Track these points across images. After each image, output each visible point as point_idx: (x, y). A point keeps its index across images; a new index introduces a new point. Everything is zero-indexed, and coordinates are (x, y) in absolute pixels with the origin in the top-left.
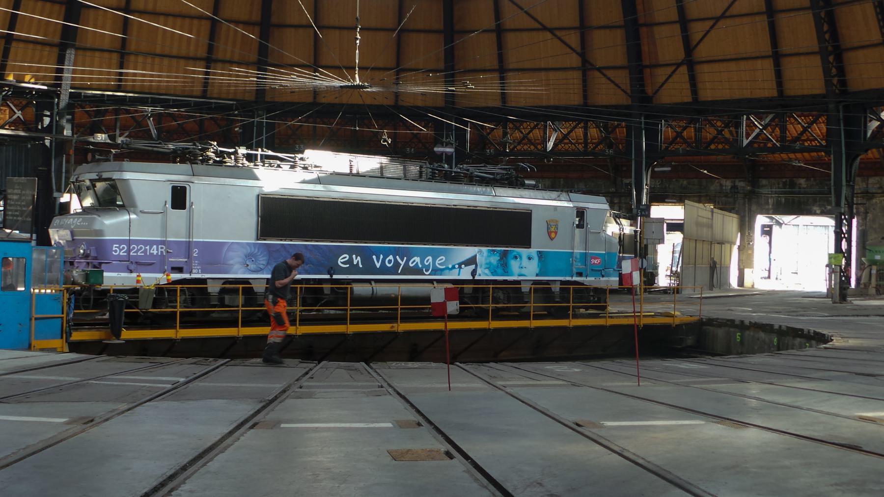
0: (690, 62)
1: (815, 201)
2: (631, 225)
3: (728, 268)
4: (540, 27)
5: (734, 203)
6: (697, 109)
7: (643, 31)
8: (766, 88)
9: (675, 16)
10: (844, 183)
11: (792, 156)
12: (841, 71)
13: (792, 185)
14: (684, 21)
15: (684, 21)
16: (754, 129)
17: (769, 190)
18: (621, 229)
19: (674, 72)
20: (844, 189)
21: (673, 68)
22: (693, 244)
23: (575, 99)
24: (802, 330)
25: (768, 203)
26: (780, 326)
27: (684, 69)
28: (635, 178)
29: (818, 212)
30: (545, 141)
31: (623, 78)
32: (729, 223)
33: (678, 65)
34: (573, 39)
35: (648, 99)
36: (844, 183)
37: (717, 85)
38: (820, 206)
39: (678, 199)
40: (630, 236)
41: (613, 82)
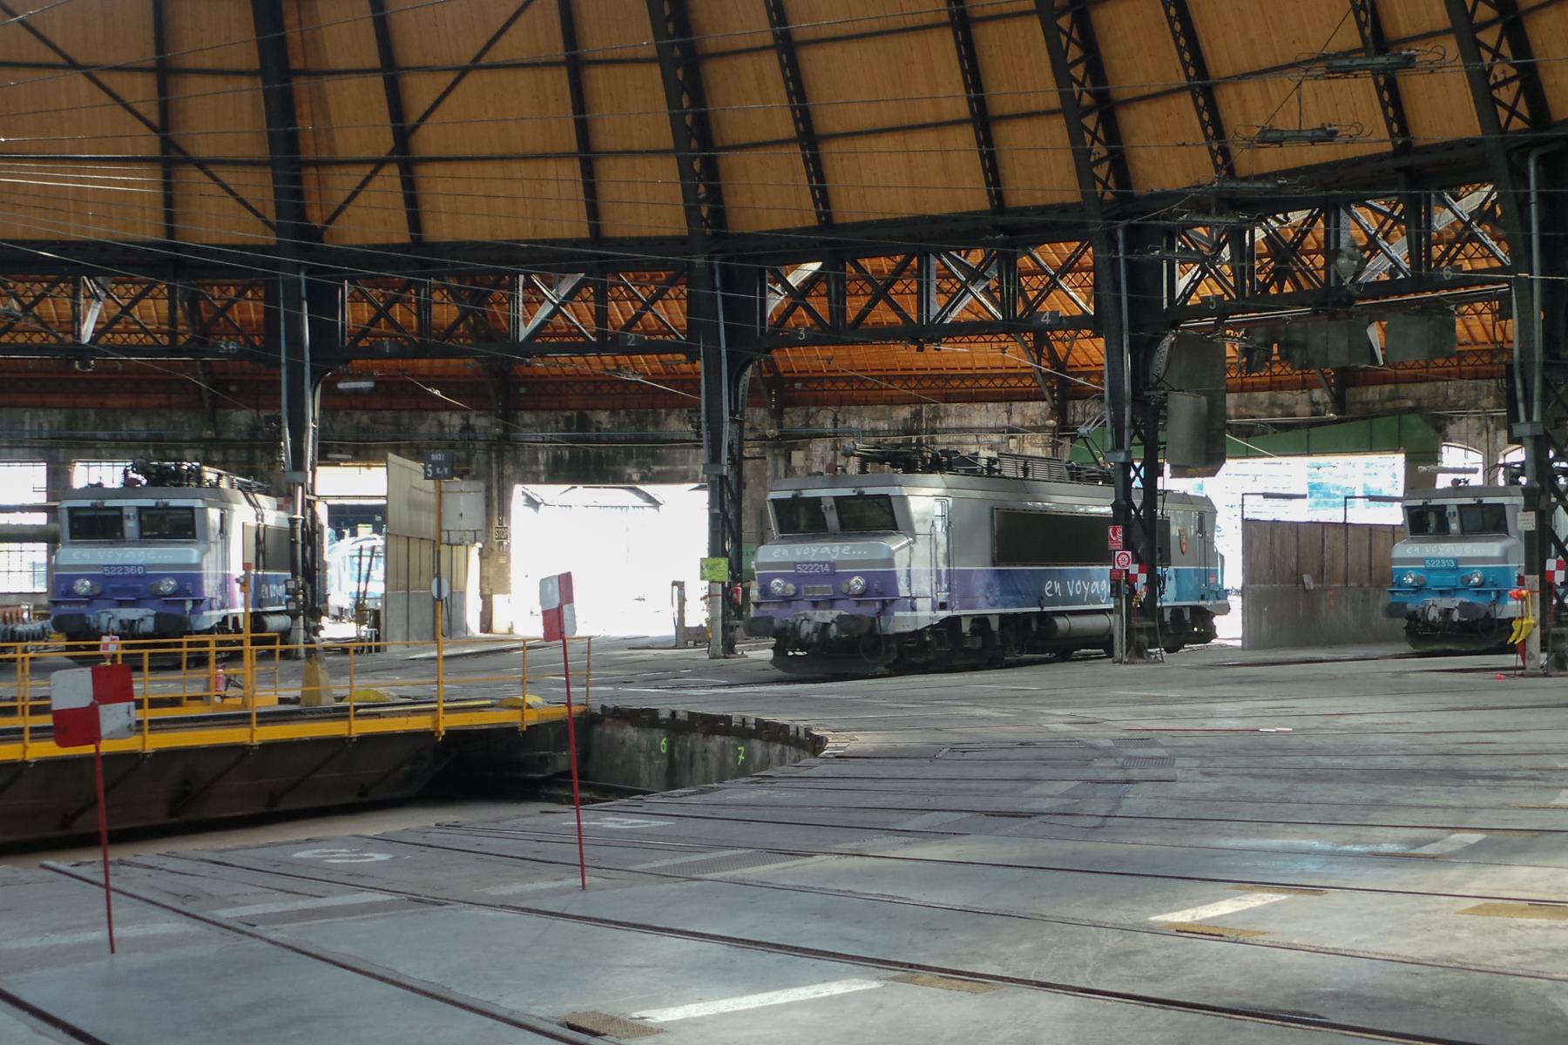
0: (404, 157)
1: (629, 455)
2: (280, 508)
3: (463, 594)
4: (60, 60)
5: (468, 462)
6: (419, 259)
7: (301, 86)
8: (569, 223)
9: (372, 58)
10: (726, 416)
11: (623, 359)
12: (716, 195)
13: (584, 423)
14: (391, 71)
15: (391, 71)
16: (536, 309)
17: (539, 433)
18: (260, 517)
19: (368, 179)
20: (727, 427)
21: (368, 169)
22: (403, 547)
23: (146, 228)
24: (728, 719)
25: (536, 461)
26: (674, 714)
27: (391, 176)
28: (289, 406)
29: (636, 477)
30: (77, 320)
31: (259, 187)
32: (465, 500)
33: (379, 164)
34: (140, 90)
35: (317, 234)
36: (726, 416)
37: (464, 211)
38: (639, 465)
39: (362, 452)
40: (278, 531)
41: (231, 193)
